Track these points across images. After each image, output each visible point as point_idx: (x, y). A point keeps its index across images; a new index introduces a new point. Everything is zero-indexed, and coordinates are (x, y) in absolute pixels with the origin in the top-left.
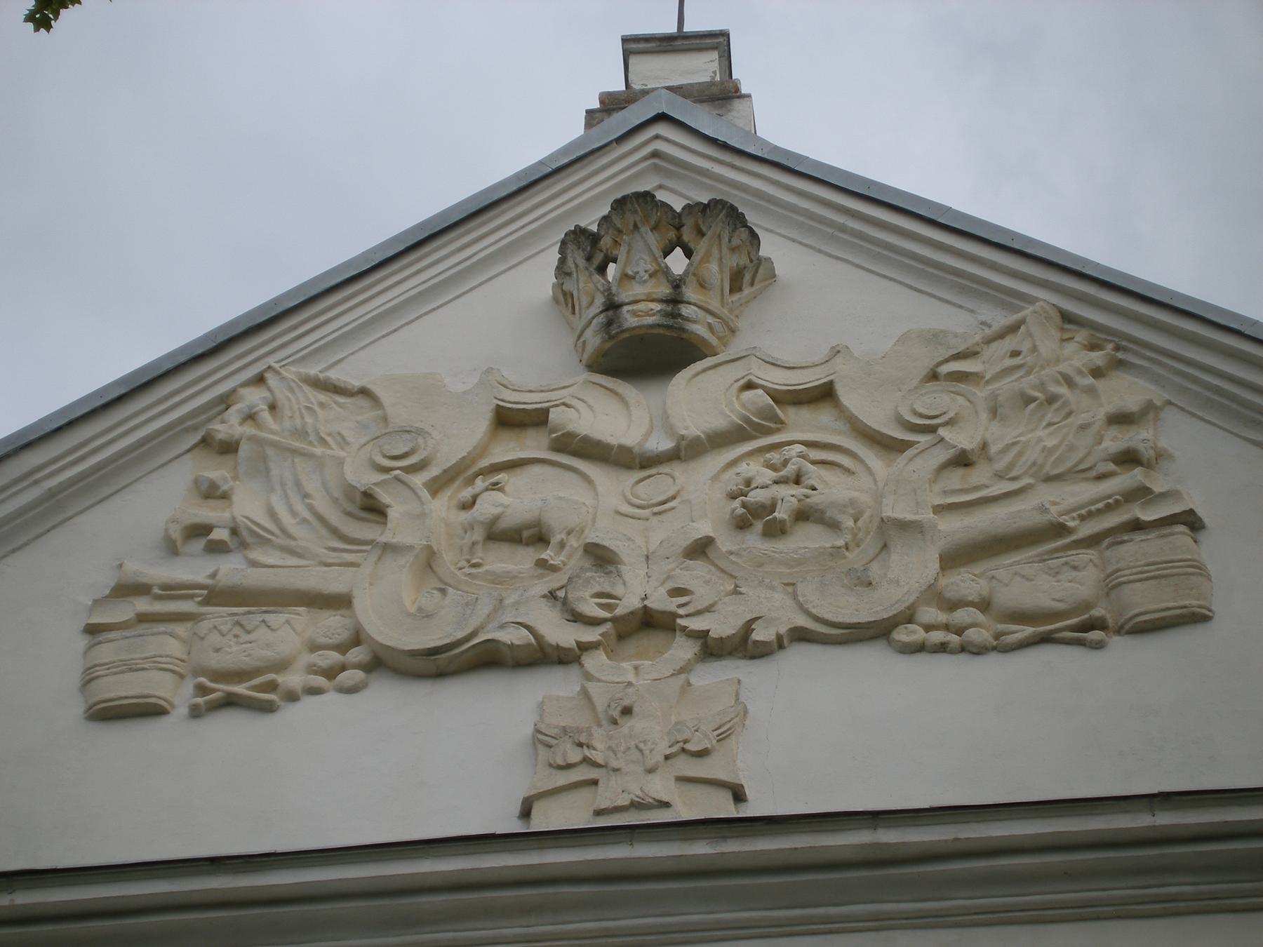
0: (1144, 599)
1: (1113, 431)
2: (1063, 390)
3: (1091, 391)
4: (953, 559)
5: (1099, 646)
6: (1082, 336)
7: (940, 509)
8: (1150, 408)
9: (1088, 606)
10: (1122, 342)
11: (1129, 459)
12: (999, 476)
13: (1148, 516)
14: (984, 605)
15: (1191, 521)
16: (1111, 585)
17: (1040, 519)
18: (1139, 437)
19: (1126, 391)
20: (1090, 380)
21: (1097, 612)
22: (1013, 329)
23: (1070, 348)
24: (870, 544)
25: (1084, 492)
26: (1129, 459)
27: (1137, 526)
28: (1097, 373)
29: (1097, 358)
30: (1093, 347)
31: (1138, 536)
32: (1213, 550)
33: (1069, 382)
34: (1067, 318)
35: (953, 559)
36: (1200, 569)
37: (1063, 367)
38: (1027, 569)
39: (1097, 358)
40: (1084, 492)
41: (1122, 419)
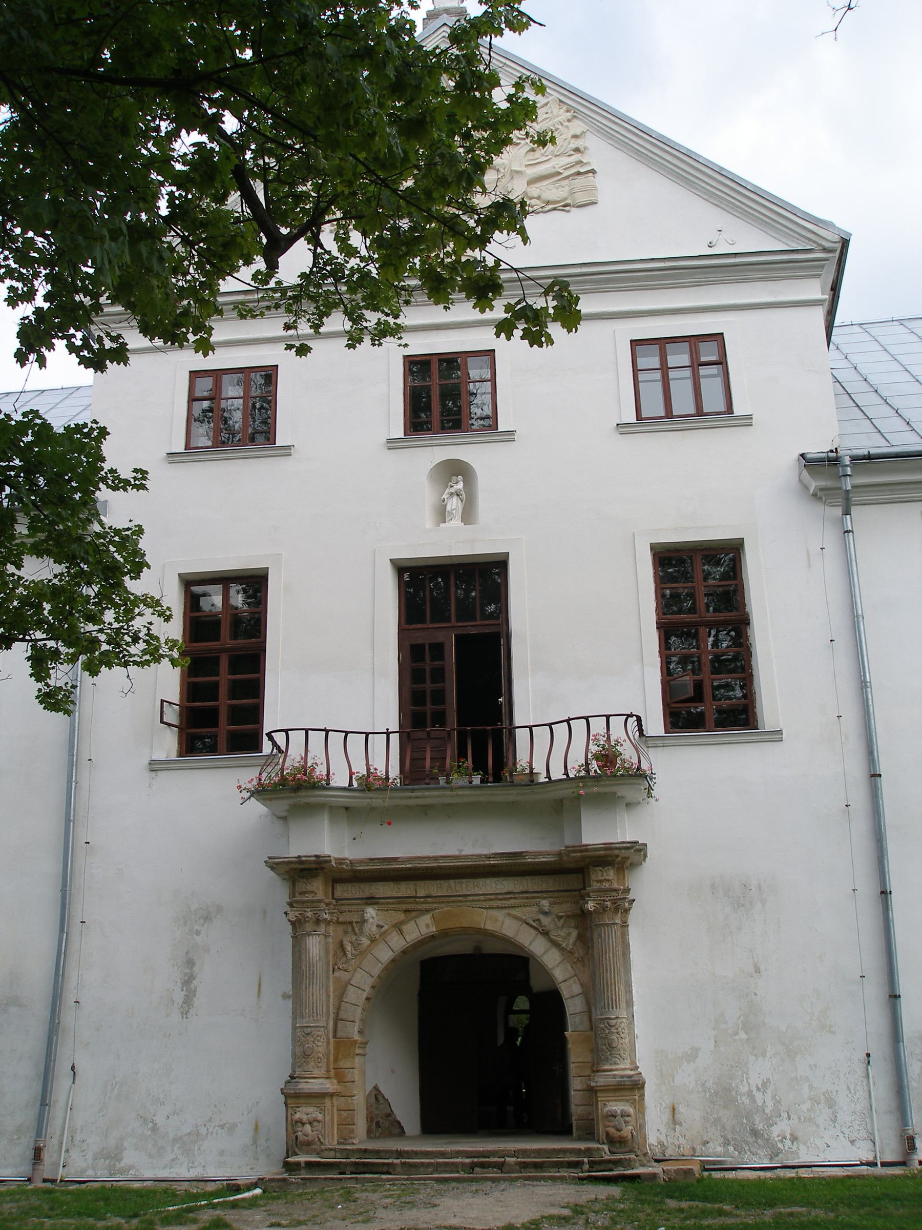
0: (581, 198)
1: (573, 141)
2: (560, 127)
3: (567, 127)
4: (530, 183)
5: (568, 211)
6: (565, 108)
7: (526, 166)
8: (583, 132)
9: (566, 199)
10: (576, 111)
11: (577, 150)
12: (543, 155)
13: (582, 170)
14: (539, 198)
15: (593, 172)
16: (572, 193)
17: (554, 170)
18: (578, 143)
19: (577, 127)
20: (567, 124)
21: (568, 201)
22: (546, 104)
23: (562, 111)
24: (508, 177)
25: (566, 160)
26: (577, 150)
27: (579, 173)
28: (569, 121)
29: (569, 115)
30: (568, 111)
31: (579, 177)
32: (599, 181)
33: (562, 124)
34: (561, 101)
35: (530, 183)
36: (595, 188)
37: (559, 119)
38: (550, 187)
39: (569, 115)
40: (566, 160)
41: (575, 137)
